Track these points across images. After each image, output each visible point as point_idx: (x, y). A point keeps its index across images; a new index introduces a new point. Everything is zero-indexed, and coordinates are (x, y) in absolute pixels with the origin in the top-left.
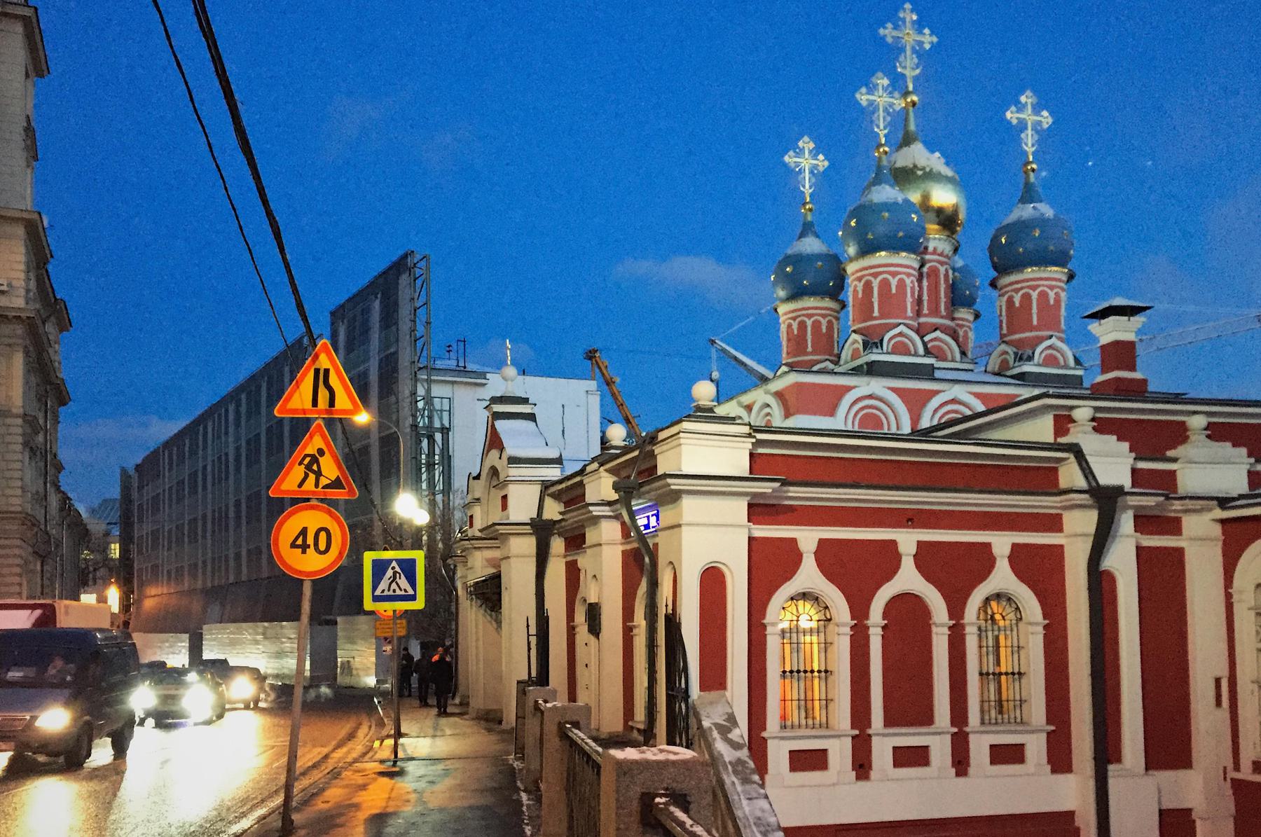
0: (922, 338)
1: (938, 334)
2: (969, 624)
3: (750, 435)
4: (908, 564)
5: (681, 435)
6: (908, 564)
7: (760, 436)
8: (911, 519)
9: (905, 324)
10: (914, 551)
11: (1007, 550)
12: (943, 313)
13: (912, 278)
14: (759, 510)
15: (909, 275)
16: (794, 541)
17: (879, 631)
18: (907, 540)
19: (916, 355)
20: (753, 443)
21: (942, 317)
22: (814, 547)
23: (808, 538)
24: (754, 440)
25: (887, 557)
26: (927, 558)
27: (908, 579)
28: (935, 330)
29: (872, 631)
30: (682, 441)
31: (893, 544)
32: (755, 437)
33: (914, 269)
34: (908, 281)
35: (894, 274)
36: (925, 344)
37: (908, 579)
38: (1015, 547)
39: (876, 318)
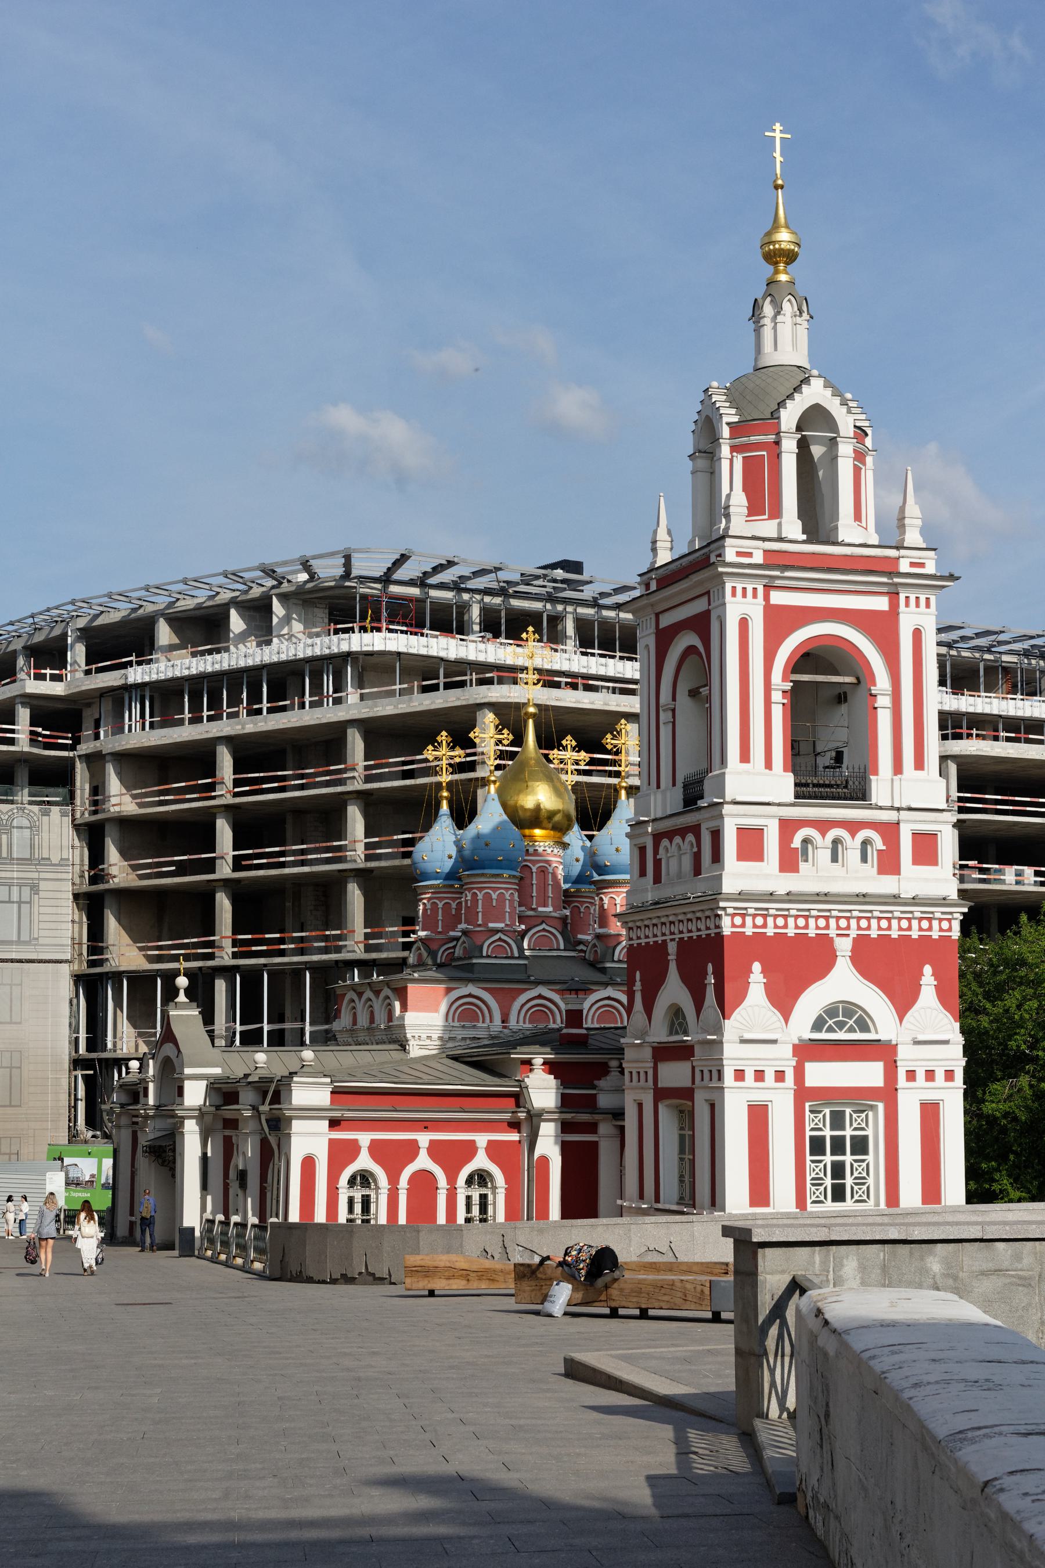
1: (544, 926)
2: (460, 1187)
4: (423, 1154)
6: (423, 1154)
7: (336, 1084)
8: (426, 1126)
10: (427, 1145)
11: (485, 1145)
14: (334, 1124)
15: (507, 889)
16: (356, 1141)
17: (406, 1191)
18: (424, 1139)
19: (512, 957)
22: (368, 1144)
23: (365, 1139)
25: (411, 1150)
26: (436, 1150)
27: (423, 1161)
28: (543, 922)
29: (400, 1191)
31: (415, 1142)
34: (507, 897)
35: (495, 889)
37: (423, 1161)
38: (489, 1142)
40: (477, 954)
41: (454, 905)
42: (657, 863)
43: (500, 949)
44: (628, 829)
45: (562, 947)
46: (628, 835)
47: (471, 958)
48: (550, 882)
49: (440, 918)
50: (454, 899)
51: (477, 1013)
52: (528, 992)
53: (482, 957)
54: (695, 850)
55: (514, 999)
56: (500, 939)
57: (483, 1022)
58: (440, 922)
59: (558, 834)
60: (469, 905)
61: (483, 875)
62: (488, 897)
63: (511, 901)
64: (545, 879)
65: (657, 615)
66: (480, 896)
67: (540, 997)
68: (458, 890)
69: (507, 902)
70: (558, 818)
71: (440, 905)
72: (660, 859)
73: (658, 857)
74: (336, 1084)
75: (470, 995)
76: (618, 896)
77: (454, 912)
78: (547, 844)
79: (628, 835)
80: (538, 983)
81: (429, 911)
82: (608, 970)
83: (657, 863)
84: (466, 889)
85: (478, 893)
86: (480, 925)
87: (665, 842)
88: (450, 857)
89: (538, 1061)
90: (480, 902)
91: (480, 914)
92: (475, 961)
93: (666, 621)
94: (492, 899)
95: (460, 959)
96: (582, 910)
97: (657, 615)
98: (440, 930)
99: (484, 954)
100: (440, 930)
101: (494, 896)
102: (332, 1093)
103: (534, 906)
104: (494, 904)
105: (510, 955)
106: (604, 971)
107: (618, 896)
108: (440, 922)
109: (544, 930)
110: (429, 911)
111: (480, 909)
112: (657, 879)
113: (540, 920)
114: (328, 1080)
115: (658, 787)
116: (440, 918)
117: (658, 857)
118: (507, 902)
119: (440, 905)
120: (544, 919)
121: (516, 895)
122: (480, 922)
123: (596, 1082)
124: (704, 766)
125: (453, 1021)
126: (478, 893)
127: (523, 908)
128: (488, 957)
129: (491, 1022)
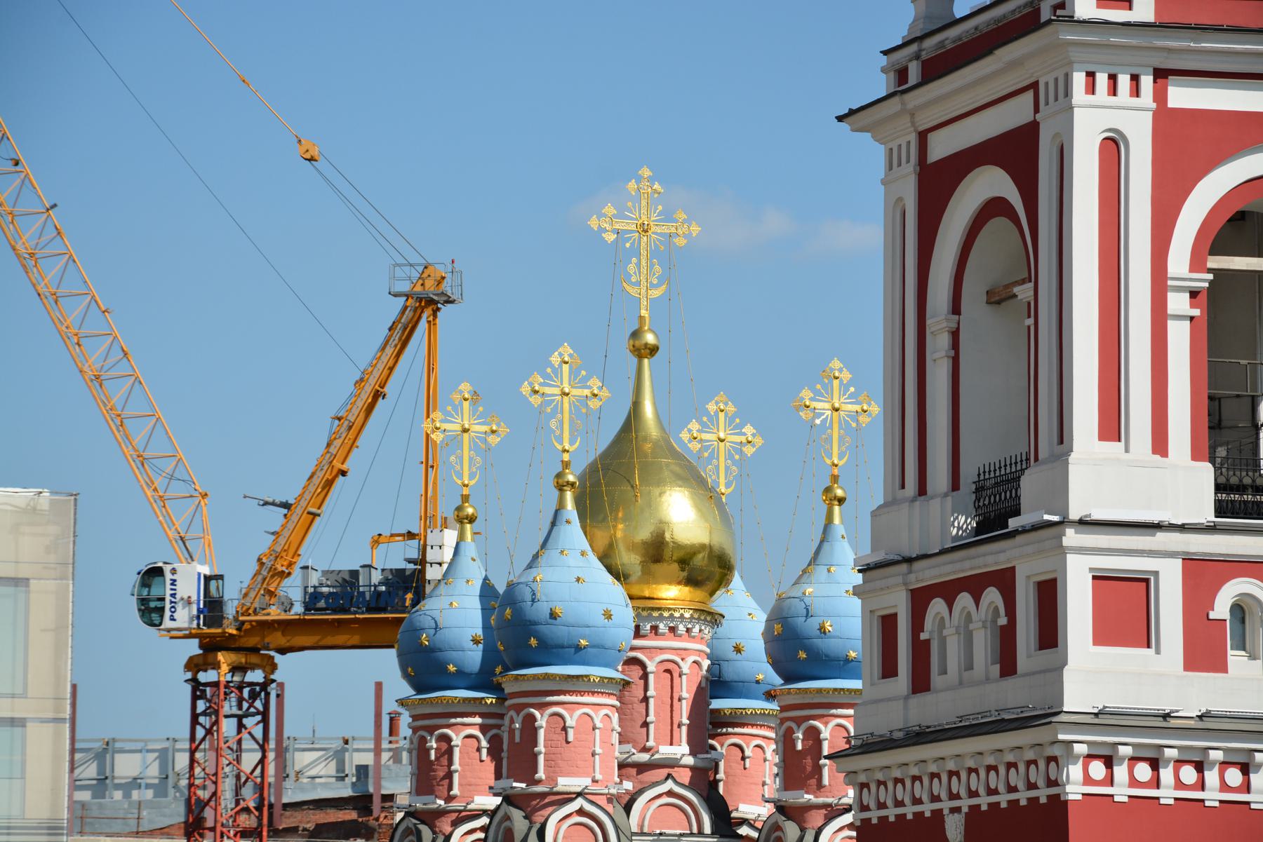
13: (605, 711)
42: (921, 651)
44: (859, 579)
46: (857, 591)
54: (1003, 621)
56: (581, 812)
59: (699, 594)
60: (517, 739)
65: (923, 137)
66: (542, 719)
68: (493, 710)
70: (700, 560)
72: (928, 642)
73: (923, 636)
76: (826, 724)
79: (857, 591)
83: (921, 651)
84: (510, 708)
85: (537, 714)
86: (539, 782)
87: (937, 606)
88: (476, 642)
90: (541, 733)
93: (941, 147)
97: (923, 137)
103: (651, 743)
109: (670, 793)
111: (541, 747)
112: (921, 683)
115: (922, 490)
117: (923, 636)
121: (615, 718)
122: (541, 774)
124: (1020, 448)
127: (628, 747)
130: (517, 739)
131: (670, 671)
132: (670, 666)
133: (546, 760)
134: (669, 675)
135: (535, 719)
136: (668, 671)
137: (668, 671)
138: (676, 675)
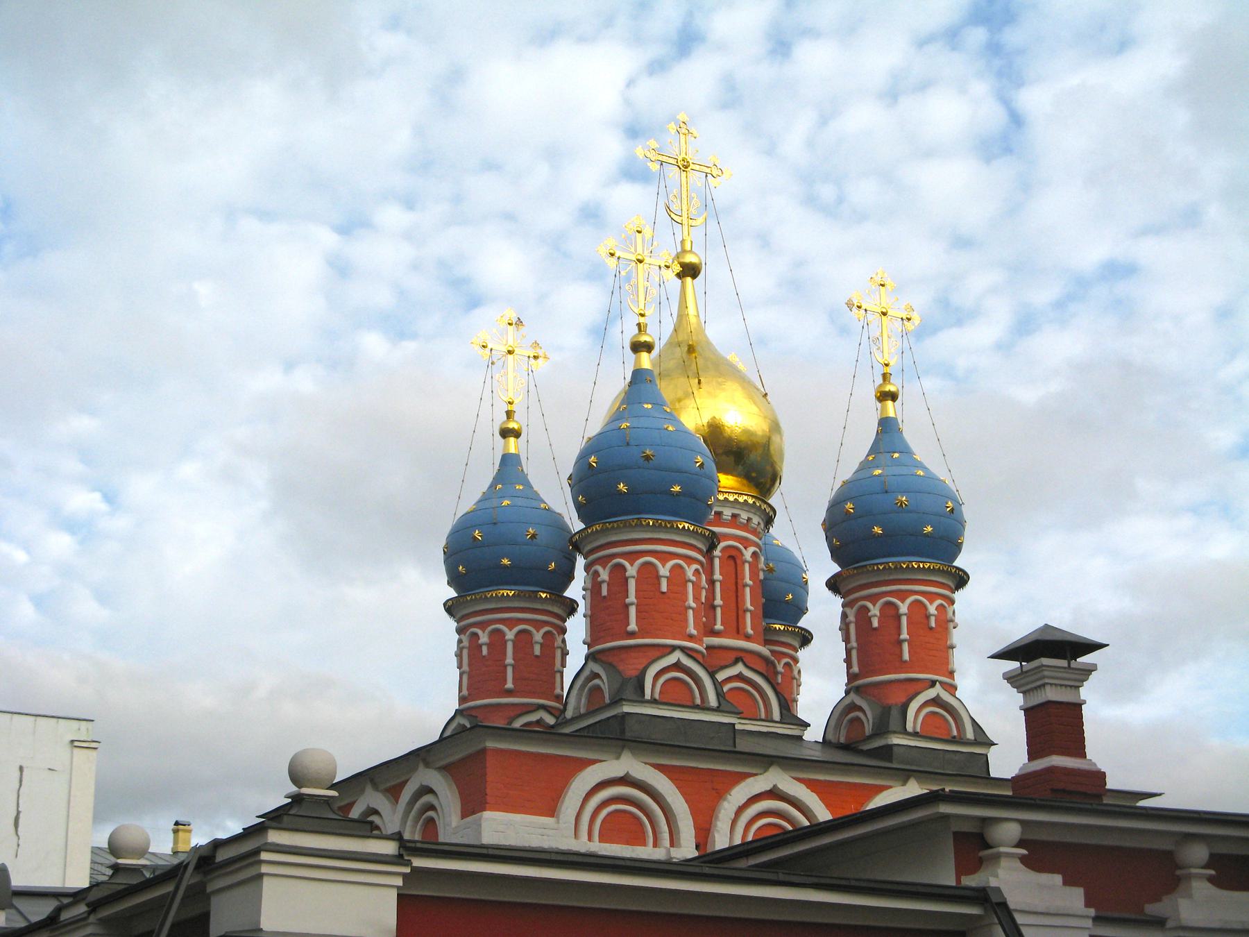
0: (712, 675)
1: (739, 668)
3: (398, 859)
5: (264, 856)
7: (419, 862)
9: (683, 650)
12: (750, 631)
13: (695, 566)
19: (704, 708)
20: (404, 876)
21: (748, 638)
24: (407, 870)
30: (264, 869)
32: (408, 863)
33: (699, 550)
34: (690, 571)
35: (664, 557)
36: (718, 686)
39: (632, 635)
40: (629, 693)
41: (538, 636)
43: (677, 693)
45: (776, 716)
47: (616, 701)
48: (748, 581)
49: (509, 660)
50: (538, 625)
51: (641, 824)
52: (750, 780)
53: (642, 701)
55: (720, 794)
56: (677, 666)
57: (655, 845)
58: (510, 671)
60: (604, 592)
61: (639, 526)
62: (649, 574)
63: (697, 586)
64: (737, 575)
66: (632, 570)
67: (774, 794)
69: (690, 586)
71: (510, 635)
74: (419, 862)
75: (625, 780)
76: (903, 601)
77: (537, 650)
78: (741, 499)
80: (767, 761)
81: (485, 651)
82: (895, 749)
85: (627, 564)
86: (632, 635)
89: (1008, 831)
91: (633, 611)
92: (627, 708)
94: (658, 577)
95: (580, 717)
96: (780, 668)
98: (509, 685)
99: (648, 696)
100: (509, 685)
101: (664, 571)
102: (403, 900)
104: (664, 588)
105: (698, 701)
106: (887, 752)
107: (903, 601)
108: (510, 671)
110: (485, 651)
111: (632, 598)
113: (733, 656)
114: (389, 848)
116: (509, 660)
118: (690, 586)
119: (510, 635)
120: (740, 656)
122: (633, 626)
123: (1152, 909)
125: (590, 838)
126: (627, 564)
128: (654, 701)
129: (672, 845)
130: (604, 592)
131: (733, 557)
132: (734, 553)
133: (638, 611)
134: (732, 562)
135: (625, 569)
136: (732, 558)
137: (732, 558)
138: (739, 562)
